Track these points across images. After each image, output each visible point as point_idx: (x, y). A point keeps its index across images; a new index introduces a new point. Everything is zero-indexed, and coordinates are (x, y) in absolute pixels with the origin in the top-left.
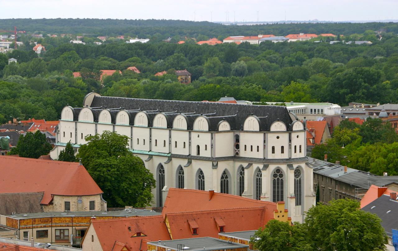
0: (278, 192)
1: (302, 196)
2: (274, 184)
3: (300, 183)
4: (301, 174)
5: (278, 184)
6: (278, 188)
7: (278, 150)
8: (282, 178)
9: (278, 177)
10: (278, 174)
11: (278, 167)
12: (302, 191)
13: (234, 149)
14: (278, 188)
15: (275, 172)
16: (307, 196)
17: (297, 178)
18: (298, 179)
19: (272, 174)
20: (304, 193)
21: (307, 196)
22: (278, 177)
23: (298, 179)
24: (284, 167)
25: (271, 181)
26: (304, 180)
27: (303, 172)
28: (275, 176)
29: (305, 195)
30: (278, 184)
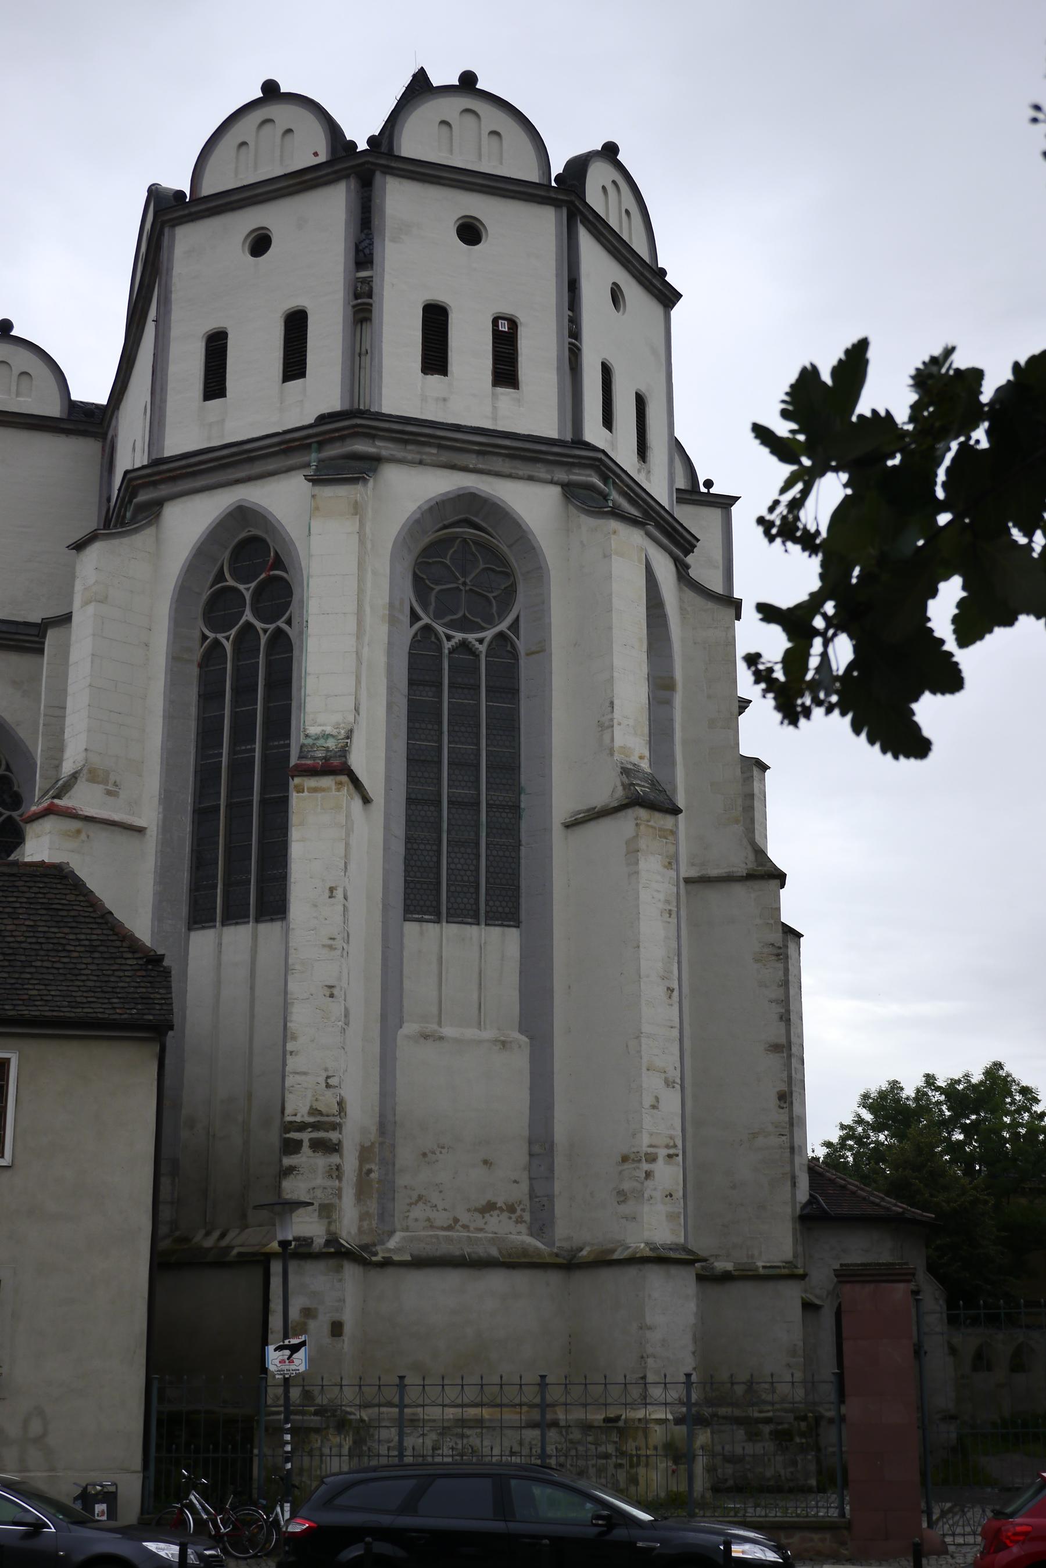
0: (241, 768)
2: (210, 696)
4: (521, 588)
5: (244, 690)
6: (243, 732)
7: (255, 355)
8: (281, 623)
9: (248, 616)
10: (247, 590)
14: (243, 732)
15: (220, 577)
17: (465, 625)
18: (481, 639)
19: (183, 592)
20: (546, 793)
22: (248, 616)
23: (481, 639)
25: (175, 659)
26: (542, 649)
28: (219, 607)
30: (244, 690)
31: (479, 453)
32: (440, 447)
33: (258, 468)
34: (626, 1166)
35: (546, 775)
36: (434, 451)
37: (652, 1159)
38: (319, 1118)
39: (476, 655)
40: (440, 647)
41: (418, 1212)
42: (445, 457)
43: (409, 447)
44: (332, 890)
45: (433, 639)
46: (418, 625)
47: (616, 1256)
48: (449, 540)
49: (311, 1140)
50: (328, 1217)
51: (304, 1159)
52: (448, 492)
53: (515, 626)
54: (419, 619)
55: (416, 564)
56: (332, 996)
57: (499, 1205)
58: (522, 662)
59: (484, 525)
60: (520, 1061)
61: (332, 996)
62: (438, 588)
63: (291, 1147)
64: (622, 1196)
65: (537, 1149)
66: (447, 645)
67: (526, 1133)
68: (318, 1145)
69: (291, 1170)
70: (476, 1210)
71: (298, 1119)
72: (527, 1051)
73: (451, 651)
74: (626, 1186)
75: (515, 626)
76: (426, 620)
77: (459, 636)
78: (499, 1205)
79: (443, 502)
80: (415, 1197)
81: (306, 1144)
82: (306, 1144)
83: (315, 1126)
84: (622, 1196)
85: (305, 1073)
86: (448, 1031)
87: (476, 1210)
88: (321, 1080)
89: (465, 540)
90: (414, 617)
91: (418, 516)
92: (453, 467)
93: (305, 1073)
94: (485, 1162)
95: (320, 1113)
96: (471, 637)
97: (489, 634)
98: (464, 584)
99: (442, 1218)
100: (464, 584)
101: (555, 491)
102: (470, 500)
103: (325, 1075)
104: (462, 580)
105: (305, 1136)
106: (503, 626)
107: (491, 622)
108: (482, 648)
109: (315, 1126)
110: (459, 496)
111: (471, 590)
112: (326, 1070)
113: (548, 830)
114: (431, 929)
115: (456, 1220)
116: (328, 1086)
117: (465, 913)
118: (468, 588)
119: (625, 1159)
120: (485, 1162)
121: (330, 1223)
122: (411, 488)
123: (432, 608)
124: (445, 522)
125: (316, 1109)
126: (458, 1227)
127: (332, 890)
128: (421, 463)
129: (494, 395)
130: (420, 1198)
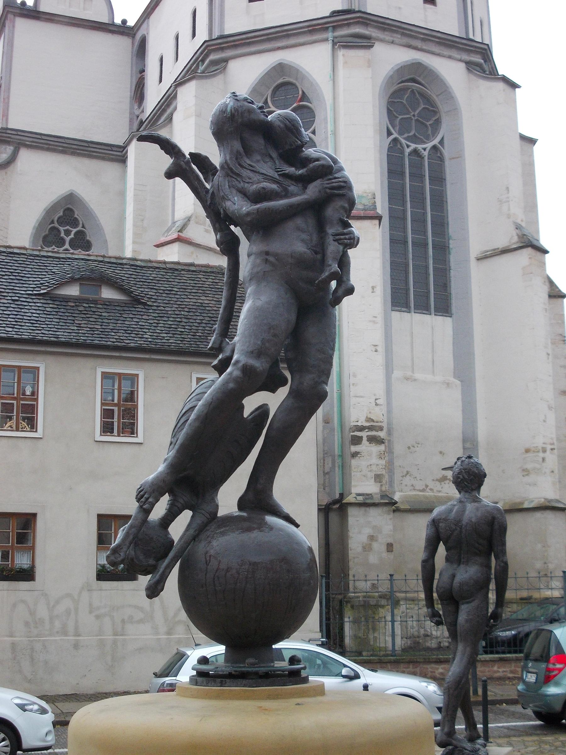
1: (453, 259)
3: (439, 179)
11: (280, 68)
12: (453, 229)
13: (131, 113)
16: (483, 257)
17: (414, 139)
18: (425, 148)
20: (465, 239)
21: (483, 257)
23: (425, 148)
24: (312, 61)
26: (459, 157)
27: (455, 110)
29: (476, 246)
31: (423, 40)
32: (403, 34)
33: (292, 41)
34: (528, 455)
35: (464, 229)
36: (399, 36)
37: (544, 451)
38: (372, 424)
39: (422, 157)
40: (402, 152)
41: (407, 481)
42: (405, 40)
43: (386, 33)
44: (373, 288)
45: (399, 146)
46: (392, 137)
47: (526, 506)
48: (404, 89)
49: (367, 436)
50: (380, 482)
51: (364, 448)
52: (407, 61)
53: (442, 142)
54: (392, 134)
55: (388, 102)
56: (376, 351)
57: (448, 478)
58: (447, 163)
59: (423, 82)
60: (456, 394)
61: (376, 351)
62: (401, 117)
63: (357, 441)
64: (526, 472)
65: (468, 445)
66: (407, 151)
67: (461, 436)
68: (372, 439)
69: (355, 455)
70: (437, 480)
71: (359, 424)
72: (460, 388)
73: (410, 154)
74: (529, 466)
75: (442, 142)
76: (395, 135)
77: (413, 146)
78: (448, 478)
79: (405, 66)
80: (405, 473)
81: (365, 439)
82: (365, 439)
83: (370, 428)
84: (526, 472)
85: (362, 397)
86: (417, 376)
87: (437, 480)
88: (373, 400)
89: (413, 91)
90: (389, 133)
91: (392, 73)
92: (409, 46)
93: (362, 397)
94: (441, 453)
95: (373, 421)
96: (420, 147)
97: (429, 145)
98: (414, 116)
99: (420, 485)
100: (414, 116)
101: (462, 66)
102: (418, 66)
103: (374, 398)
104: (413, 113)
105: (364, 434)
106: (436, 142)
107: (428, 138)
108: (426, 153)
109: (370, 428)
110: (413, 64)
111: (417, 120)
112: (375, 395)
113: (467, 261)
114: (406, 316)
115: (427, 486)
116: (376, 404)
117: (423, 307)
118: (416, 118)
119: (527, 451)
120: (441, 453)
121: (381, 485)
122: (391, 56)
123: (397, 128)
124: (403, 79)
125: (370, 418)
126: (428, 490)
127: (373, 288)
128: (393, 42)
129: (425, 8)
130: (408, 473)
